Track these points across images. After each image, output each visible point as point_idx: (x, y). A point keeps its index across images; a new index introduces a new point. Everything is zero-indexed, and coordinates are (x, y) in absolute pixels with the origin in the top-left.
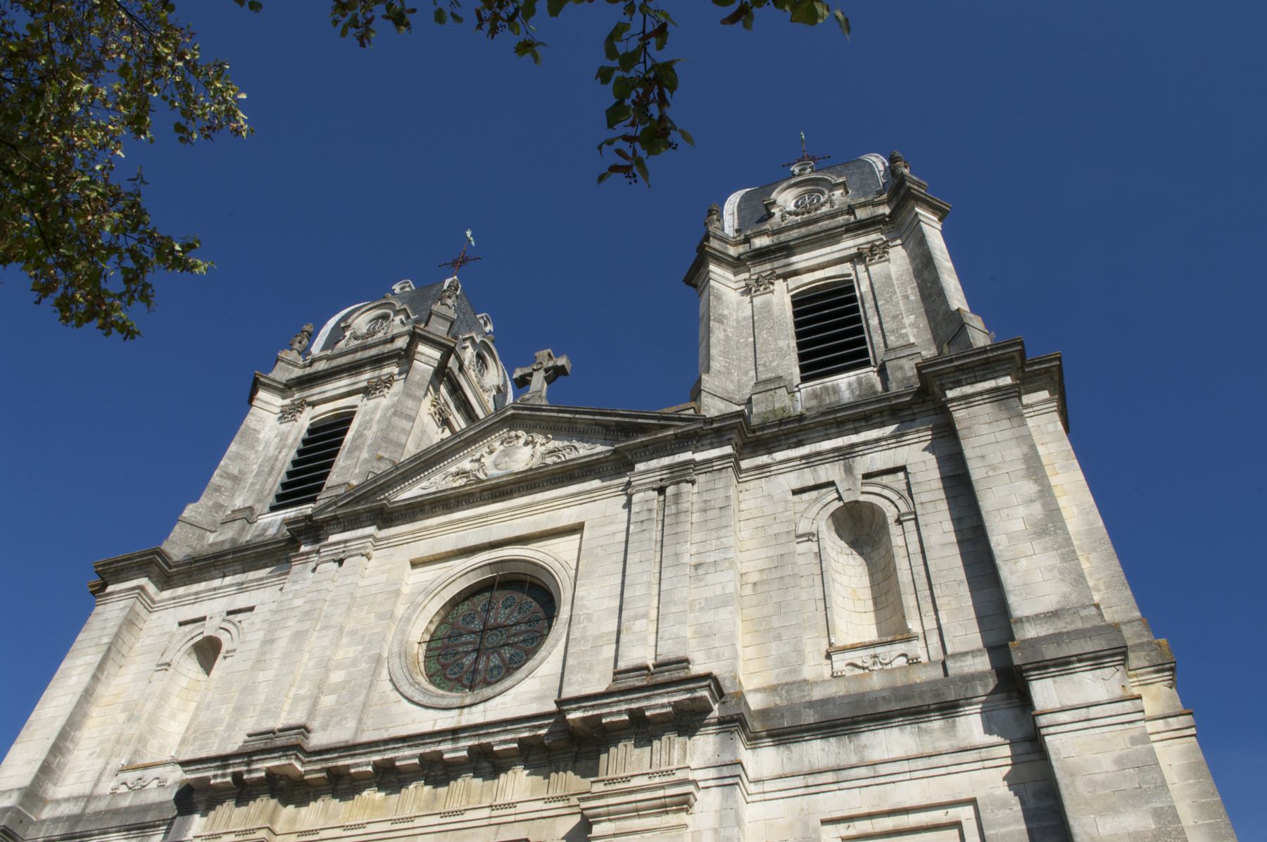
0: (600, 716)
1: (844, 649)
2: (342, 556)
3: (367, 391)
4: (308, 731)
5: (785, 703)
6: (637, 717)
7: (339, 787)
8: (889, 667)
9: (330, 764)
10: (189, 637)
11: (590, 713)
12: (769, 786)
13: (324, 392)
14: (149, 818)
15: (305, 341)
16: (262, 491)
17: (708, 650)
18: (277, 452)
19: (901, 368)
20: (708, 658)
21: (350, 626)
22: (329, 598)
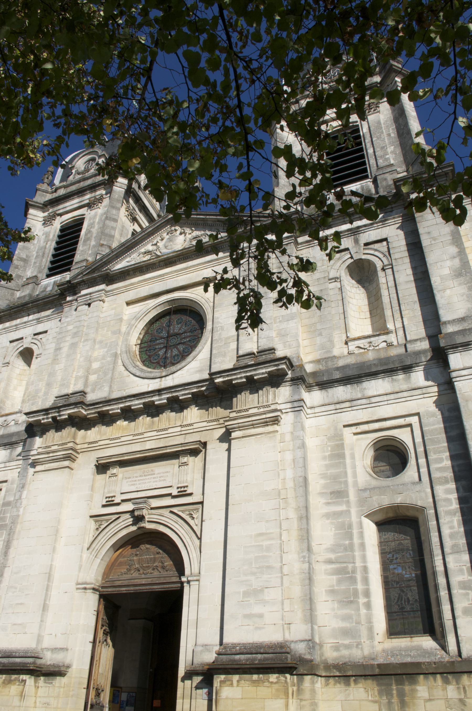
0: (232, 380)
1: (354, 339)
2: (89, 302)
3: (89, 205)
4: (85, 394)
5: (324, 368)
6: (250, 379)
7: (105, 420)
8: (377, 348)
9: (99, 410)
10: (16, 348)
11: (226, 379)
12: (317, 410)
13: (65, 207)
14: (14, 439)
15: (50, 177)
16: (40, 266)
17: (284, 343)
18: (45, 244)
19: (386, 179)
20: (285, 347)
21: (99, 338)
22: (85, 324)
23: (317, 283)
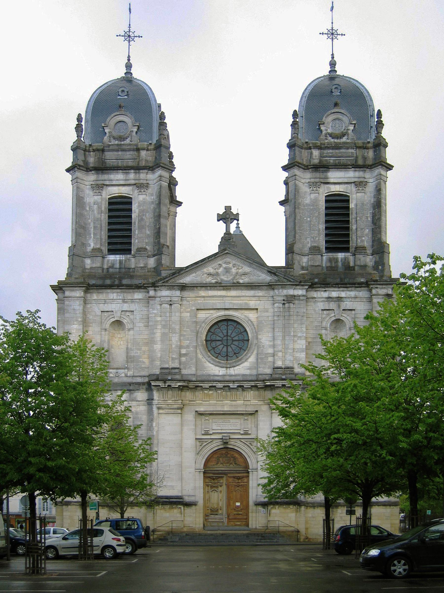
23: (315, 328)
